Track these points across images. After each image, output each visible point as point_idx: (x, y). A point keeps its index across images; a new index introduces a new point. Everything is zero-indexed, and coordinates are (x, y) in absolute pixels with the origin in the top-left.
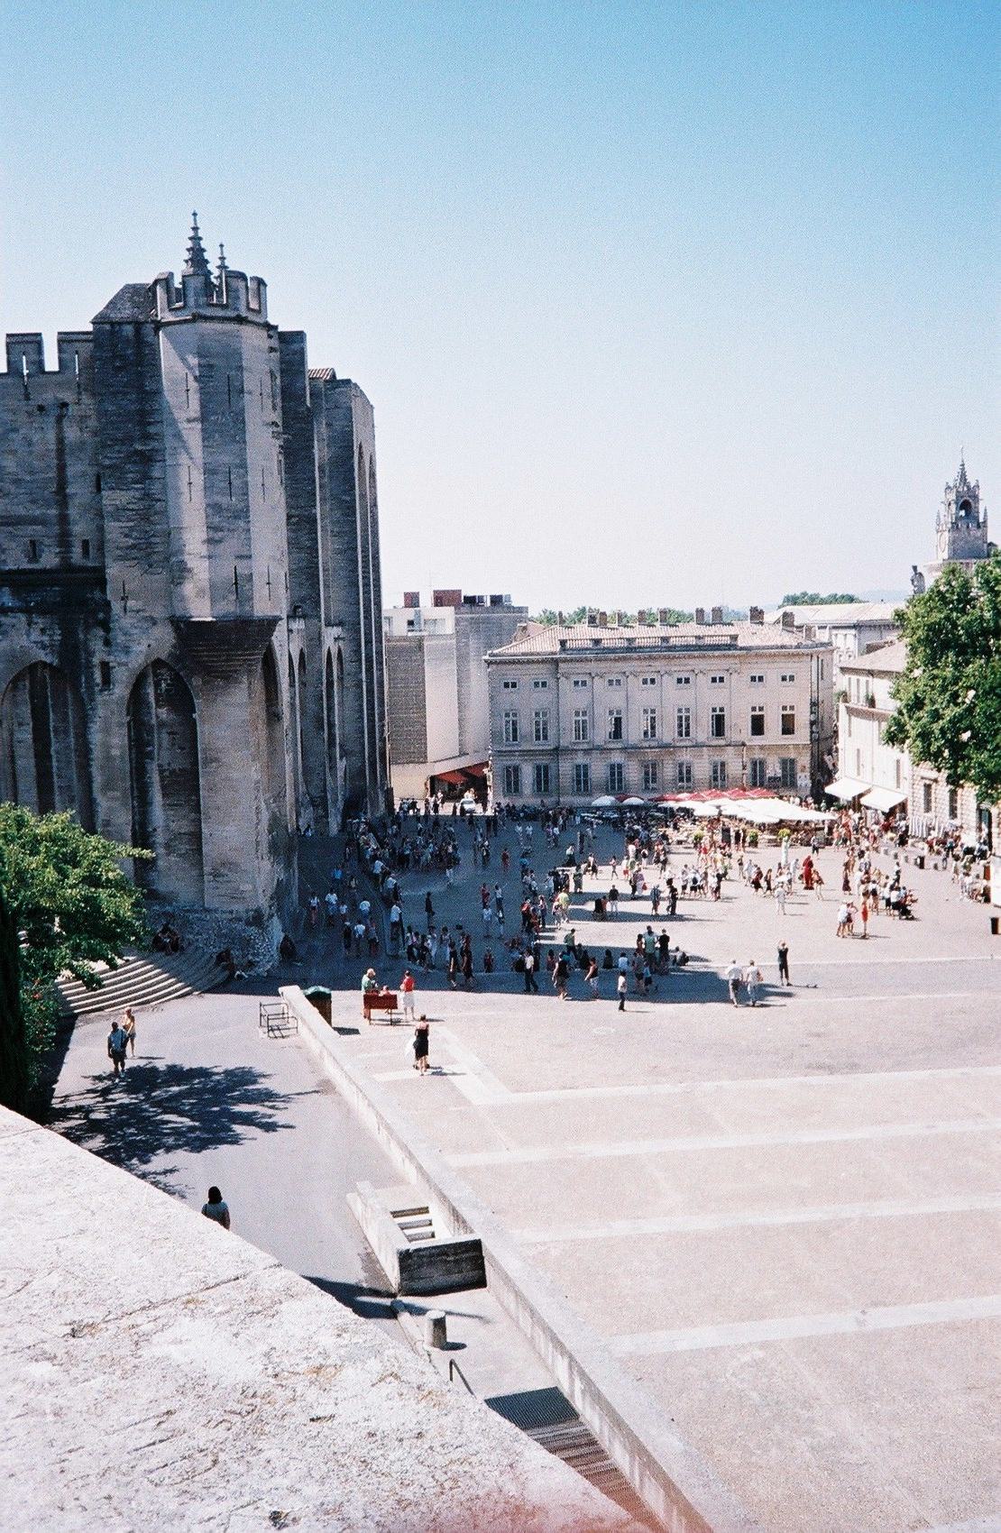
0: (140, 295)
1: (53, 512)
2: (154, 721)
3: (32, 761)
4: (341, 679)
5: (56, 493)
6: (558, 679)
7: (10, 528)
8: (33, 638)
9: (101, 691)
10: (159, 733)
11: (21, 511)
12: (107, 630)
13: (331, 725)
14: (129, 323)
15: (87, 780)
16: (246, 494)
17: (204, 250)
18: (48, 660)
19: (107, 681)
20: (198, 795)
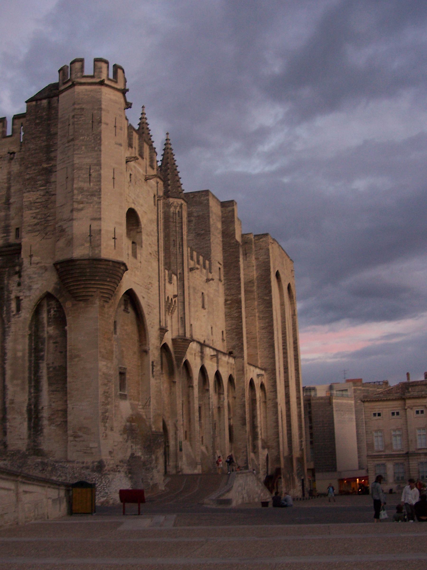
2: (46, 335)
5: (5, 203)
6: (406, 409)
10: (48, 343)
12: (20, 277)
13: (254, 427)
14: (45, 98)
16: (100, 181)
19: (19, 309)
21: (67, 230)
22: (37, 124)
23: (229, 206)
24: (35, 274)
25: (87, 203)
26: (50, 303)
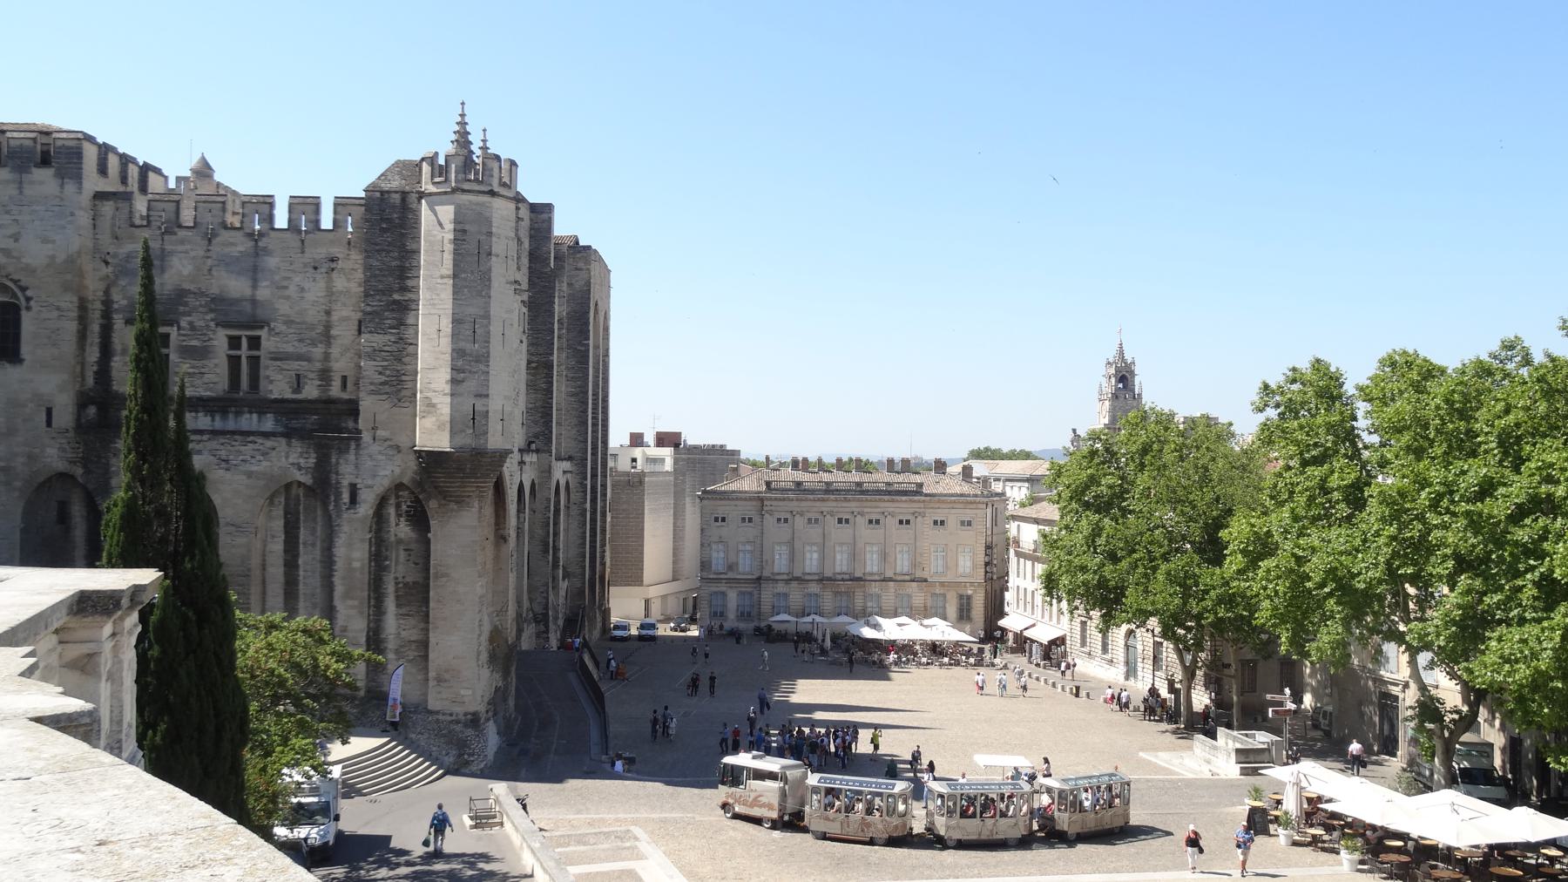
0: (410, 169)
1: (318, 351)
2: (393, 539)
3: (281, 570)
4: (567, 508)
7: (278, 363)
8: (291, 460)
9: (347, 509)
10: (397, 550)
11: (289, 348)
13: (556, 549)
15: (329, 588)
16: (489, 342)
17: (469, 133)
18: (303, 479)
19: (354, 500)
20: (428, 607)
21: (439, 406)
22: (384, 230)
23: (542, 213)
24: (380, 453)
25: (470, 372)
26: (401, 493)
